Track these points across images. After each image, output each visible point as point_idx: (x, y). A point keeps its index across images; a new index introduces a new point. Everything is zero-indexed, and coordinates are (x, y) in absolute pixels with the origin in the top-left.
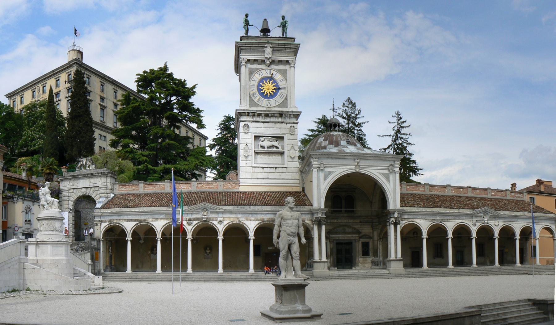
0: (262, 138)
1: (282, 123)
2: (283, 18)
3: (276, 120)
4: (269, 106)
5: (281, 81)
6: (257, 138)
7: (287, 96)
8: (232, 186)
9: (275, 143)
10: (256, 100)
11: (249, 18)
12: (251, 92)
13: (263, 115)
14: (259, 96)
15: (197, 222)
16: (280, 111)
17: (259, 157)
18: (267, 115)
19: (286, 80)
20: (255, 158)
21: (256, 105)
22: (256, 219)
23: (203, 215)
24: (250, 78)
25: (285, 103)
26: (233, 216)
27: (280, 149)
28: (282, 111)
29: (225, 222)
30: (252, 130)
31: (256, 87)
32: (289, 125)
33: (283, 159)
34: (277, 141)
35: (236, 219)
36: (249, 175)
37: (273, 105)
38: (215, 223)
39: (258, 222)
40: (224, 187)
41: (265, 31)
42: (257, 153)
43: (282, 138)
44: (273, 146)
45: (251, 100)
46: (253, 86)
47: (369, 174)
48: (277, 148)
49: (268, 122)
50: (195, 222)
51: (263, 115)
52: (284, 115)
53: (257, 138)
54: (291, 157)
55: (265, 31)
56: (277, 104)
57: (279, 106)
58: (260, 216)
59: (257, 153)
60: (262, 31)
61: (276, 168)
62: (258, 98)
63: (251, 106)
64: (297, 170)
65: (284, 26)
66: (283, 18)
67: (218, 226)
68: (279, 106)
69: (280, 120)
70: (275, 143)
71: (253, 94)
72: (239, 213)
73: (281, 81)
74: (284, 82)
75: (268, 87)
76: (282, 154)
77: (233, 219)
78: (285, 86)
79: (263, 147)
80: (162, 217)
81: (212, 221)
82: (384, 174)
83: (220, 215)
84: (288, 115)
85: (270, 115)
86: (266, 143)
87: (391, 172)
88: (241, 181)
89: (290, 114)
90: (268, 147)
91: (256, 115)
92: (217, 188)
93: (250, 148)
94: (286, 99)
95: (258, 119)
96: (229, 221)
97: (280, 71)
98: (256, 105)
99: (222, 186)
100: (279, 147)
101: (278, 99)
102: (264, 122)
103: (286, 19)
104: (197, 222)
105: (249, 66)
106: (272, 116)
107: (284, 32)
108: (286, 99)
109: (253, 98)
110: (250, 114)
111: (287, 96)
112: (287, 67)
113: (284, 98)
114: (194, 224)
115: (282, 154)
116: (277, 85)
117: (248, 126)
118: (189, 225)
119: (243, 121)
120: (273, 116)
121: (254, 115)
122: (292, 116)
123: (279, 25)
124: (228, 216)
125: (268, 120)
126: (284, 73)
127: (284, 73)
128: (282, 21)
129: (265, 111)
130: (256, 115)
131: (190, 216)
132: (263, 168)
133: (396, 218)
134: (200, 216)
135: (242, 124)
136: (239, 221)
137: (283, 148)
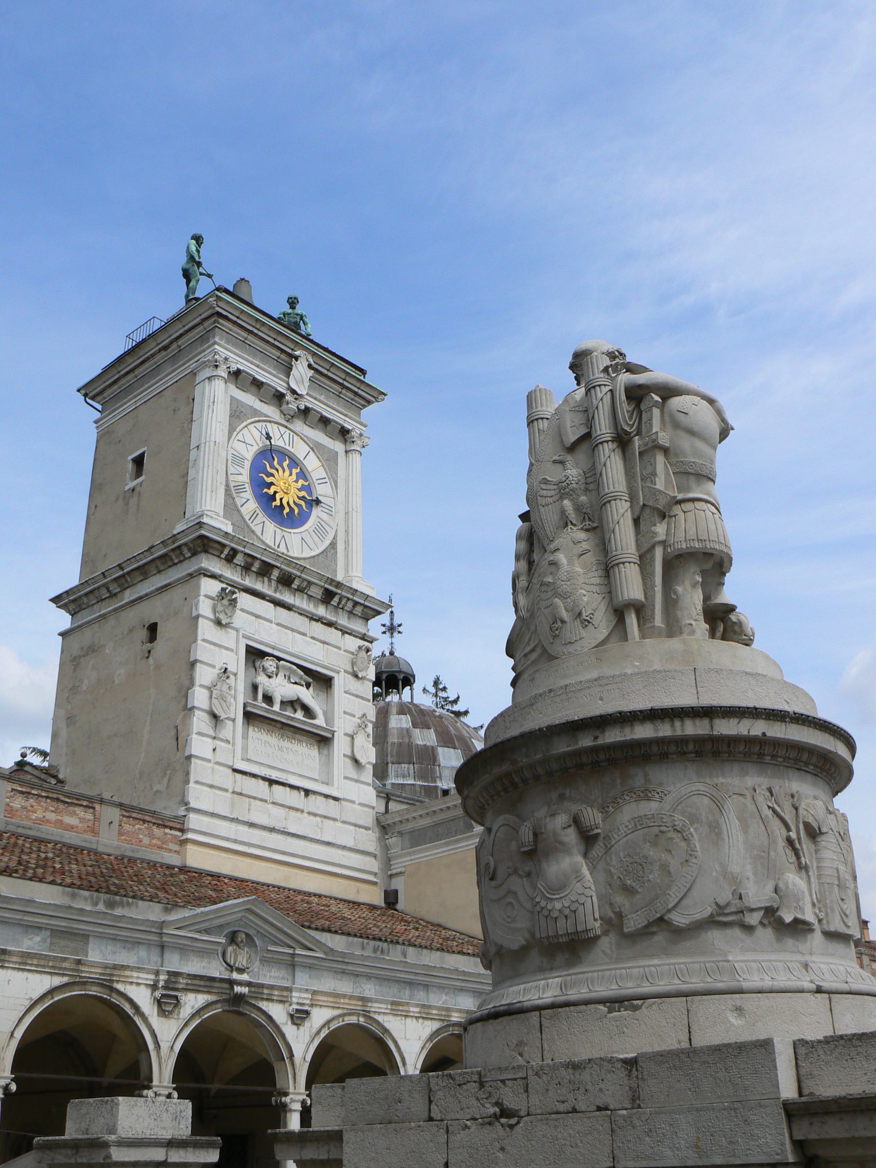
0: (270, 664)
1: (330, 624)
3: (310, 607)
6: (255, 655)
8: (152, 836)
12: (231, 478)
13: (275, 574)
15: (201, 999)
17: (259, 737)
18: (286, 581)
23: (231, 968)
24: (232, 430)
26: (345, 987)
27: (320, 721)
29: (319, 1016)
30: (239, 619)
31: (247, 465)
33: (328, 763)
34: (308, 686)
35: (357, 1005)
38: (278, 1012)
40: (120, 834)
42: (249, 717)
46: (238, 460)
49: (288, 607)
50: (192, 1002)
51: (275, 574)
53: (255, 655)
54: (356, 761)
58: (438, 999)
61: (307, 792)
64: (368, 818)
67: (289, 1030)
70: (307, 695)
71: (240, 488)
72: (369, 977)
76: (323, 740)
79: (268, 699)
80: (32, 943)
81: (264, 1005)
83: (302, 979)
84: (350, 605)
86: (282, 688)
88: (194, 821)
89: (356, 603)
91: (256, 566)
92: (94, 831)
94: (333, 545)
97: (316, 447)
104: (201, 999)
106: (300, 590)
108: (333, 545)
110: (239, 559)
112: (338, 446)
113: (327, 543)
114: (186, 1011)
115: (323, 740)
116: (308, 489)
118: (163, 1013)
119: (213, 576)
122: (359, 610)
124: (328, 983)
125: (287, 597)
127: (329, 460)
129: (289, 563)
131: (174, 962)
132: (272, 782)
134: (216, 969)
135: (209, 587)
136: (367, 1015)
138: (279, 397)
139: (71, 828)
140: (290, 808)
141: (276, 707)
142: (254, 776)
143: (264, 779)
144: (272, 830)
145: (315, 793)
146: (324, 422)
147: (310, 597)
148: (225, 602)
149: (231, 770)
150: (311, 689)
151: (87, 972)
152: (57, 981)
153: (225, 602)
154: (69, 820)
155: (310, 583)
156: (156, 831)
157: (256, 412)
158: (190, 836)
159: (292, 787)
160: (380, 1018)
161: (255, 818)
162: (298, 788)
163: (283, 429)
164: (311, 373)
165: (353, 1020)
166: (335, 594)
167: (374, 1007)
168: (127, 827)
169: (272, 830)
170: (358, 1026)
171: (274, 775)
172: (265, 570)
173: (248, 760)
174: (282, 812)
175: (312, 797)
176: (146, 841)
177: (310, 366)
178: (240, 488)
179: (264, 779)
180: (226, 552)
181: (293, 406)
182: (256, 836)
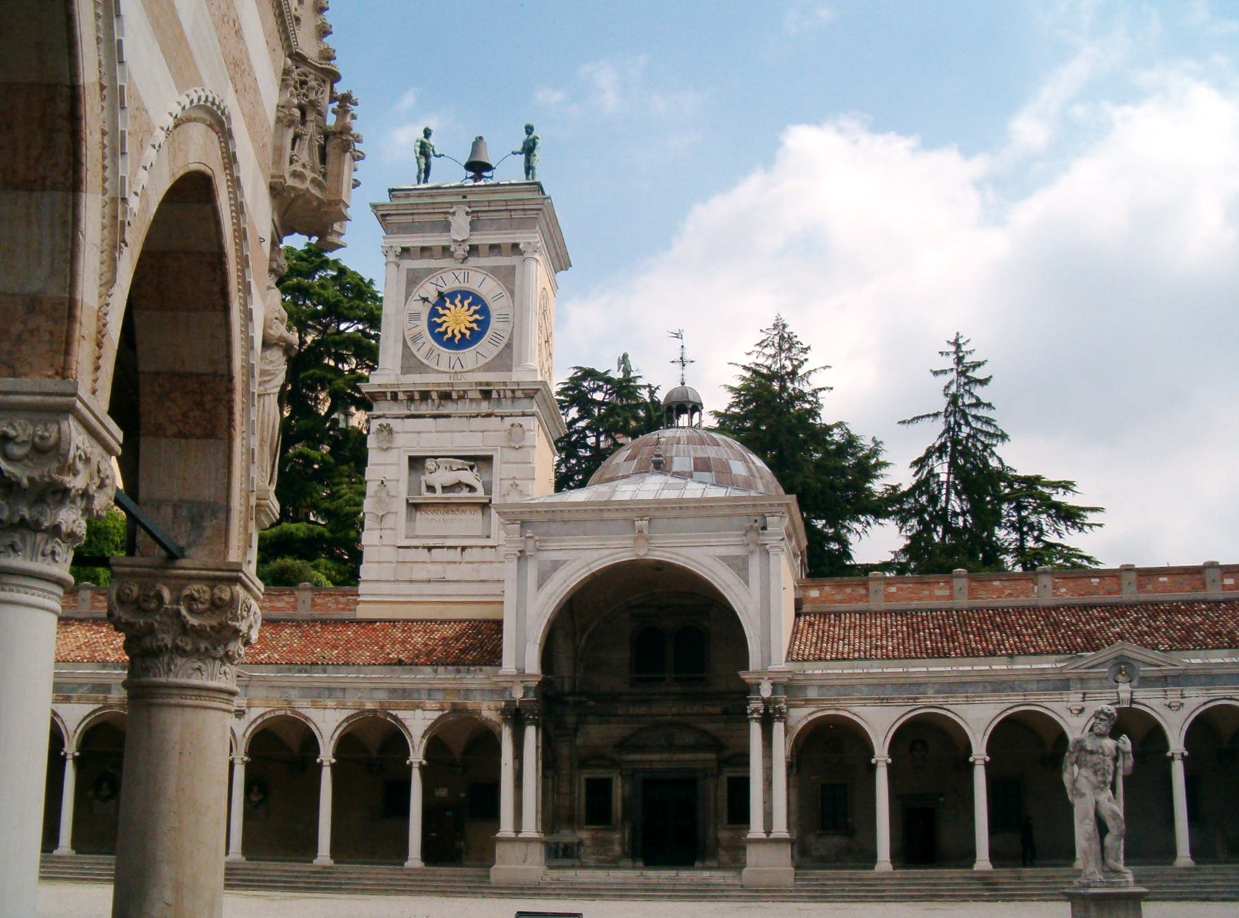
0: (430, 464)
1: (489, 415)
2: (529, 129)
3: (474, 409)
4: (458, 368)
5: (500, 296)
6: (416, 463)
7: (511, 339)
8: (338, 602)
9: (468, 477)
10: (420, 356)
11: (432, 141)
13: (434, 395)
14: (430, 341)
16: (481, 384)
17: (420, 516)
18: (445, 396)
19: (512, 294)
20: (410, 519)
21: (422, 368)
22: (341, 706)
25: (505, 359)
28: (488, 384)
29: (254, 713)
30: (400, 440)
32: (508, 421)
34: (472, 468)
36: (387, 572)
37: (468, 367)
39: (346, 713)
40: (314, 605)
41: (478, 167)
42: (414, 507)
43: (488, 460)
44: (459, 485)
45: (407, 354)
46: (415, 316)
47: (680, 561)
48: (472, 488)
49: (448, 416)
51: (434, 395)
52: (494, 395)
53: (416, 463)
55: (478, 167)
56: (482, 361)
57: (487, 368)
59: (414, 507)
60: (470, 166)
61: (464, 548)
62: (427, 347)
63: (406, 370)
65: (529, 149)
66: (529, 129)
68: (487, 368)
69: (485, 407)
70: (468, 477)
71: (415, 339)
73: (500, 296)
74: (506, 300)
75: (458, 319)
76: (485, 506)
77: (274, 703)
78: (508, 311)
79: (431, 488)
82: (729, 561)
84: (509, 394)
85: (455, 396)
86: (441, 476)
87: (752, 552)
89: (513, 391)
90: (445, 488)
91: (417, 396)
92: (295, 608)
93: (393, 493)
94: (509, 346)
95: (423, 409)
96: (261, 711)
97: (494, 271)
98: (422, 368)
99: (309, 603)
100: (479, 486)
101: (486, 348)
102: (435, 417)
103: (535, 133)
105: (408, 264)
106: (461, 398)
107: (529, 168)
108: (509, 346)
109: (414, 349)
110: (401, 396)
111: (511, 339)
113: (502, 346)
117: (391, 431)
119: (379, 417)
120: (462, 397)
121: (411, 399)
122: (519, 394)
123: (519, 149)
125: (449, 408)
126: (507, 277)
128: (525, 137)
129: (439, 384)
130: (417, 396)
132: (430, 548)
133: (767, 702)
137: (488, 491)
138: (445, 250)
139: (279, 609)
140: (449, 562)
141: (439, 493)
142: (416, 547)
143: (424, 547)
144: (429, 581)
145: (471, 547)
146: (494, 248)
147: (471, 400)
148: (385, 433)
149: (391, 549)
150: (475, 470)
151: (110, 702)
152: (97, 706)
153: (385, 433)
154: (278, 605)
155: (465, 392)
156: (341, 599)
157: (430, 271)
158: (361, 599)
159: (449, 547)
160: (303, 711)
161: (416, 576)
162: (455, 548)
163: (457, 273)
164: (469, 218)
165: (282, 713)
166: (489, 392)
167: (297, 704)
168: (319, 601)
169: (429, 581)
170: (286, 716)
171: (431, 543)
172: (425, 396)
173: (417, 537)
174: (440, 566)
175: (468, 551)
176: (333, 606)
177: (467, 213)
178: (415, 339)
179: (424, 547)
180: (389, 396)
181: (460, 252)
182: (414, 589)
